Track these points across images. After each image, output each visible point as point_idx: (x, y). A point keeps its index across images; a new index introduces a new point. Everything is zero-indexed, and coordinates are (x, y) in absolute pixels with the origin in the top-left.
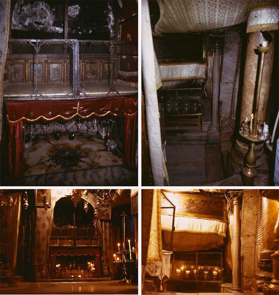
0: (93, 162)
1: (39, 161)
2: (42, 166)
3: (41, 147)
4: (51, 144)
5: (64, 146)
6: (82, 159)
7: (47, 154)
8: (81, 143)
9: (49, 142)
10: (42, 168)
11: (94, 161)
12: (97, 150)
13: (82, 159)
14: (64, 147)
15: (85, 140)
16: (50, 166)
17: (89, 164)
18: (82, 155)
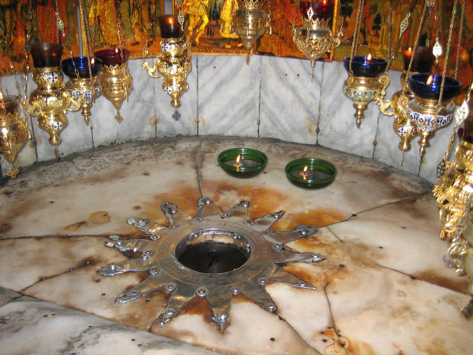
0: (331, 330)
1: (67, 228)
2: (55, 250)
3: (146, 174)
4: (199, 177)
5: (246, 198)
6: (279, 292)
7: (137, 208)
8: (346, 208)
9: (197, 168)
10: (39, 260)
11: (340, 325)
12: (411, 270)
13: (279, 292)
14: (242, 202)
15: (384, 202)
16: (88, 263)
17: (295, 333)
18: (302, 266)
